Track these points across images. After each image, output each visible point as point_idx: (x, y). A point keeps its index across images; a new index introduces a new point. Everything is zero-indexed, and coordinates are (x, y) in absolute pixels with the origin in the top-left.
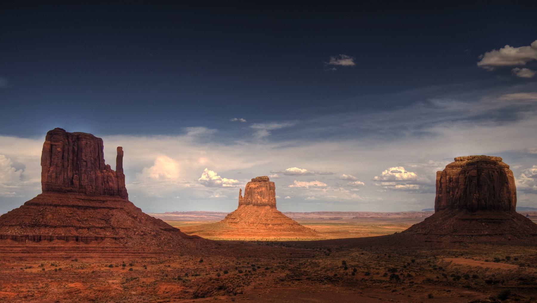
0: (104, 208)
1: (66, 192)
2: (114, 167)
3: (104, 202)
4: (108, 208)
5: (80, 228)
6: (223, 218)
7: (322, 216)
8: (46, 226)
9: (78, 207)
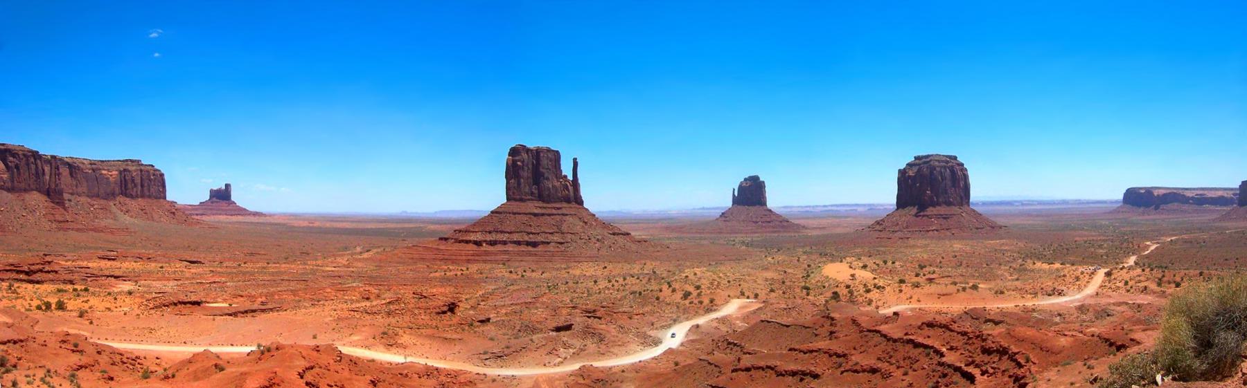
0: (559, 214)
2: (570, 178)
3: (558, 209)
4: (563, 215)
5: (533, 233)
6: (718, 217)
7: (839, 209)
8: (502, 232)
9: (535, 215)
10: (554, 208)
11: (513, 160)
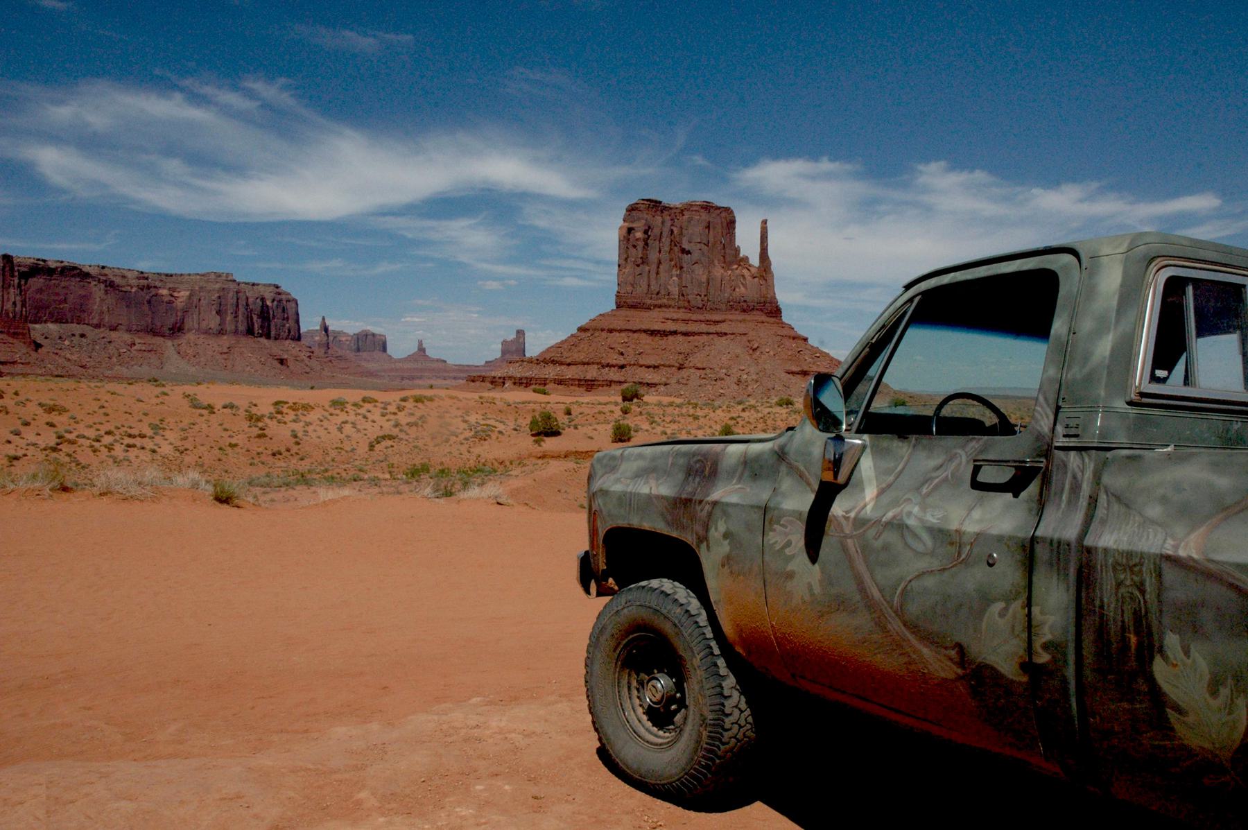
0: (708, 334)
1: (652, 308)
2: (755, 261)
3: (717, 322)
4: (717, 333)
10: (708, 322)
11: (630, 230)
